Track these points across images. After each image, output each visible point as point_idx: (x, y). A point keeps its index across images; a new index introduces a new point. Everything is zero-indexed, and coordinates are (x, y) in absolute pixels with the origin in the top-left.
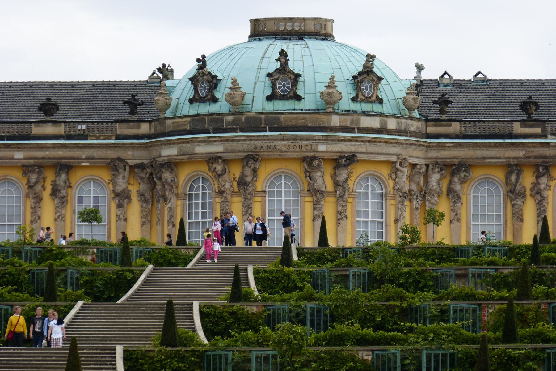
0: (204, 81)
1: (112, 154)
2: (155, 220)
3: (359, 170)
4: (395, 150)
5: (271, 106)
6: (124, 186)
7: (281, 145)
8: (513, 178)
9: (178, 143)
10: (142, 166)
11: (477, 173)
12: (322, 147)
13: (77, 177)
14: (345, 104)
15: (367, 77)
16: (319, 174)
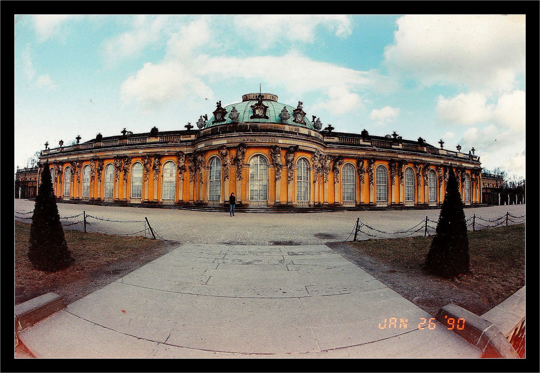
0: (220, 111)
1: (178, 149)
2: (196, 180)
3: (299, 155)
4: (315, 146)
5: (253, 120)
6: (183, 164)
7: (258, 139)
8: (361, 163)
9: (204, 141)
10: (190, 155)
11: (346, 161)
12: (281, 141)
13: (164, 160)
14: (290, 121)
15: (299, 111)
16: (279, 155)
